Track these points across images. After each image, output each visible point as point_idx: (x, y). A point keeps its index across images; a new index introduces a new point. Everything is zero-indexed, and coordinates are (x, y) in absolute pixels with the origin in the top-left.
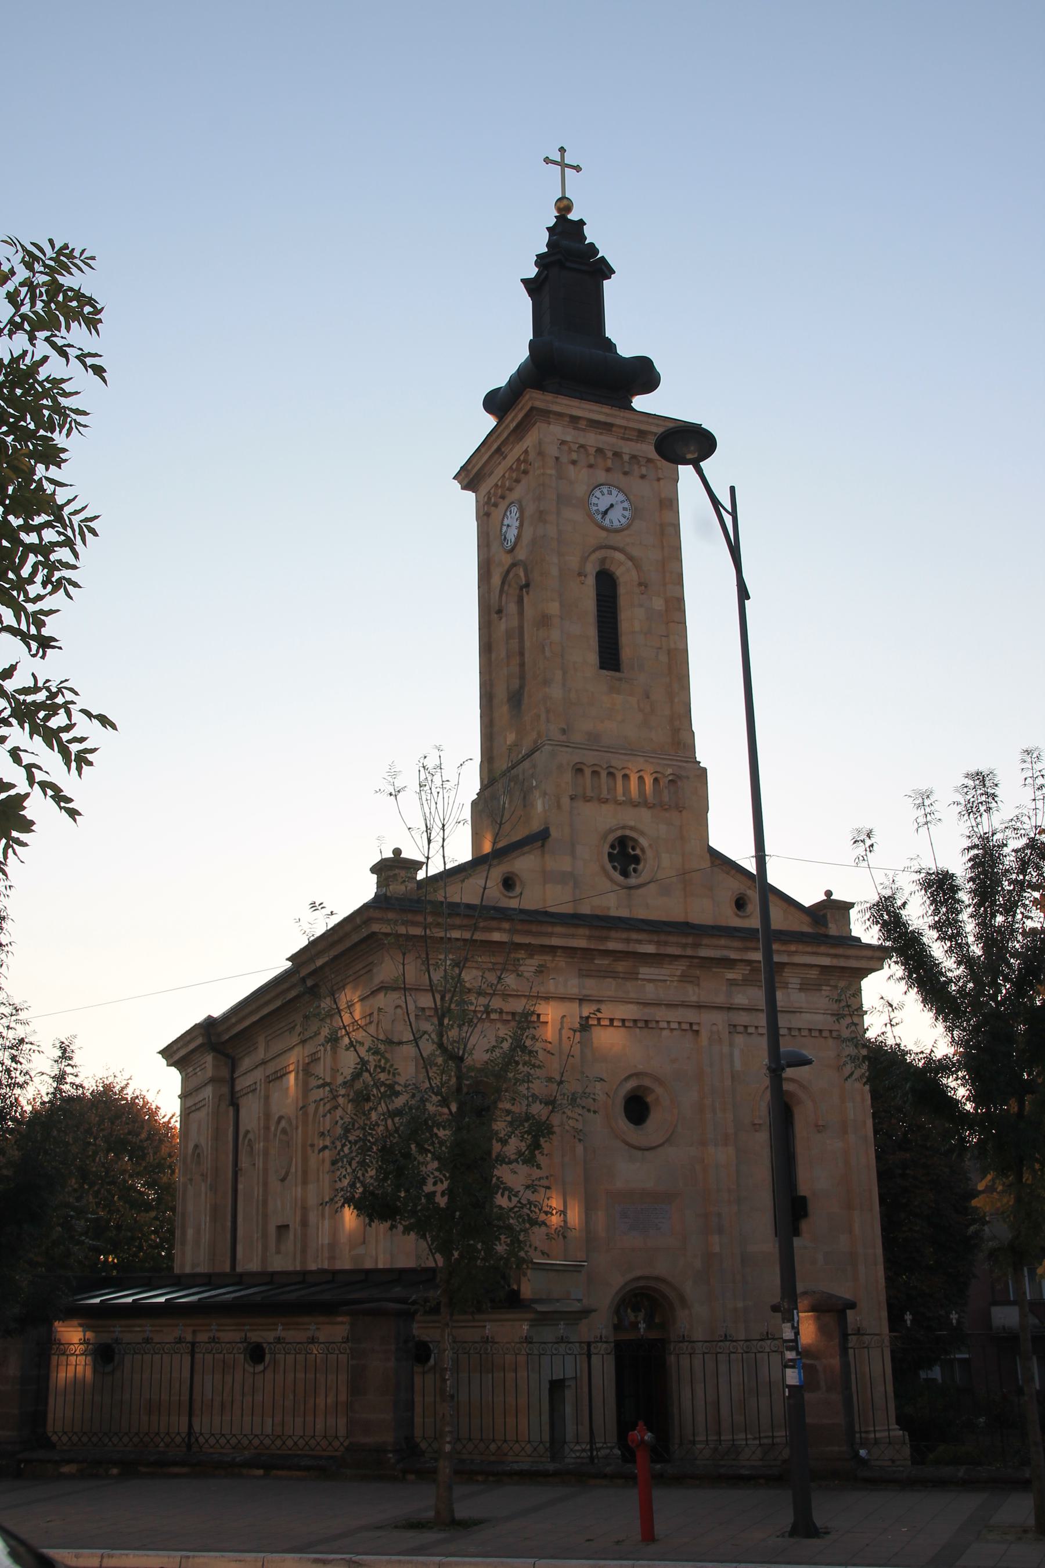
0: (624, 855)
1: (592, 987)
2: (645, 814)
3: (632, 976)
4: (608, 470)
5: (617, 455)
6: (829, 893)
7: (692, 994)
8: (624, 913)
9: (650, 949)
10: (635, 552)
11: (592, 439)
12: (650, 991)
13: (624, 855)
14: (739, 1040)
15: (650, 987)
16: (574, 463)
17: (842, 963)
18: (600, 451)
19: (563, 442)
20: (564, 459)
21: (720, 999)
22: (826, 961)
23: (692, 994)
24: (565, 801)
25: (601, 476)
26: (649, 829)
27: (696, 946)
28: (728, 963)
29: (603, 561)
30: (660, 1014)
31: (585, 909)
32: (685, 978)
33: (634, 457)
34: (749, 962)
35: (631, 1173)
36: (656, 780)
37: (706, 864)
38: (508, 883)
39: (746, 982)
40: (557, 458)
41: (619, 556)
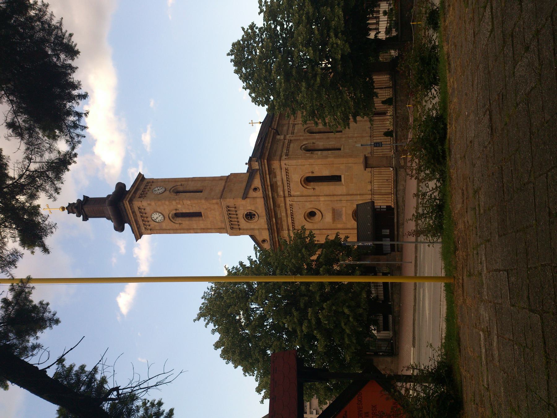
0: (250, 216)
1: (285, 227)
2: (238, 213)
3: (281, 218)
4: (147, 217)
5: (142, 216)
6: (246, 164)
7: (282, 205)
8: (265, 218)
9: (274, 220)
10: (167, 212)
11: (141, 223)
12: (284, 214)
13: (250, 216)
14: (292, 193)
15: (283, 214)
16: (149, 225)
17: (267, 172)
18: (143, 220)
19: (145, 228)
20: (150, 228)
21: (283, 199)
22: (268, 176)
23: (282, 205)
24: (241, 231)
25: (149, 219)
26: (242, 212)
27: (271, 209)
28: (273, 198)
29: (173, 218)
30: (289, 212)
31: (266, 226)
32: (279, 206)
33: (140, 212)
34: (272, 194)
35: (328, 218)
36: (229, 210)
37: (248, 200)
38: (264, 241)
39: (277, 192)
40: (151, 230)
41: (170, 215)
